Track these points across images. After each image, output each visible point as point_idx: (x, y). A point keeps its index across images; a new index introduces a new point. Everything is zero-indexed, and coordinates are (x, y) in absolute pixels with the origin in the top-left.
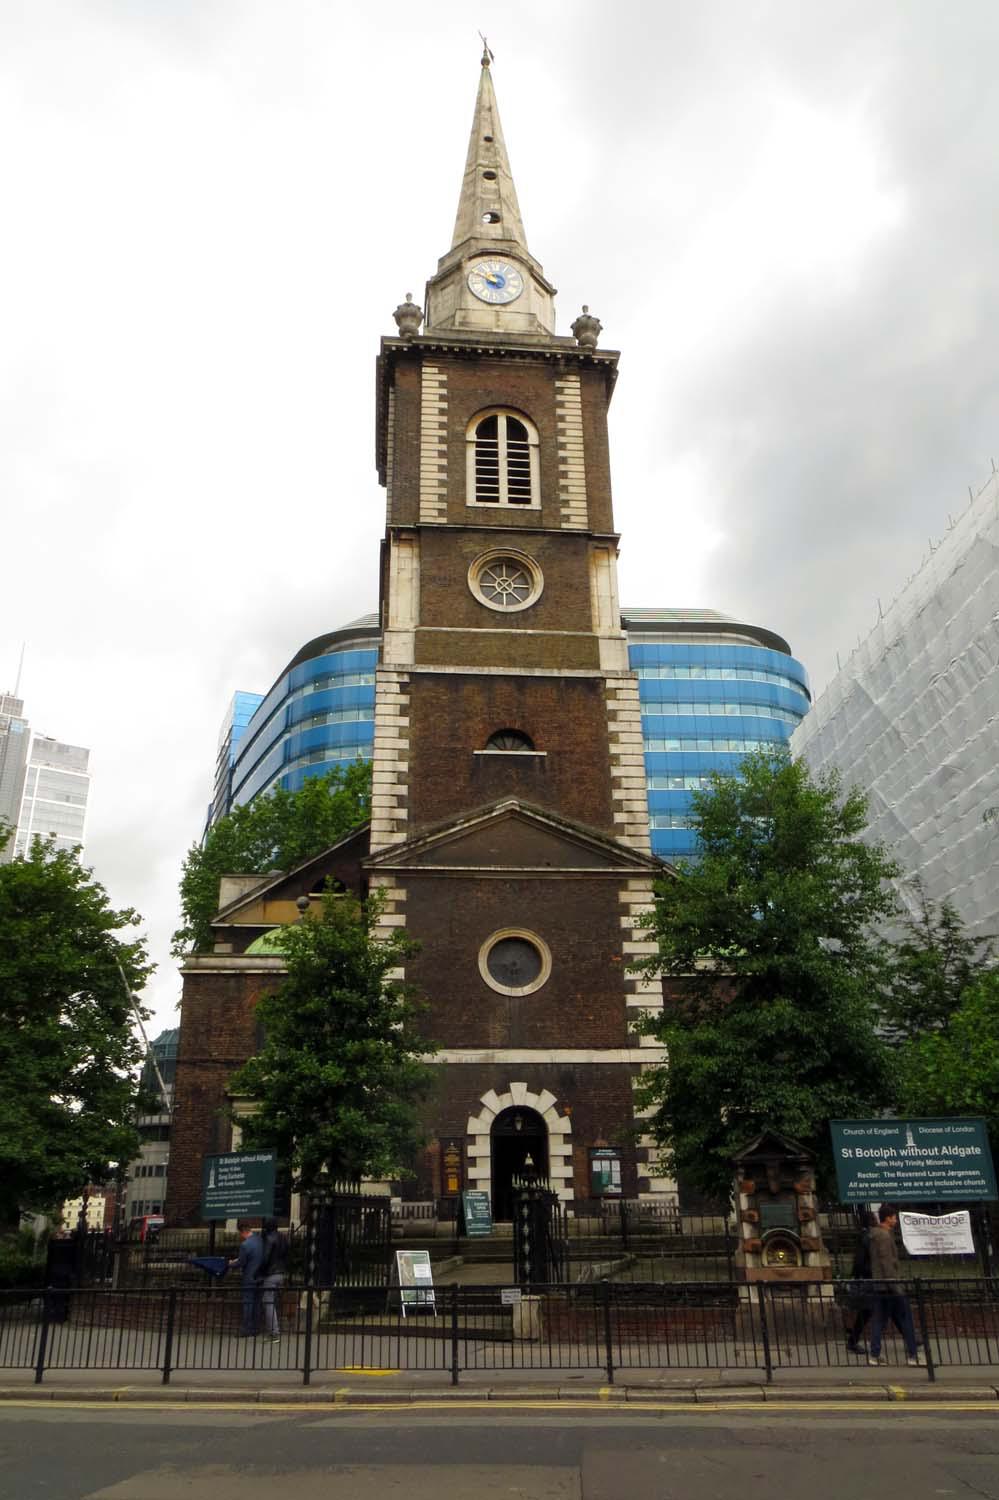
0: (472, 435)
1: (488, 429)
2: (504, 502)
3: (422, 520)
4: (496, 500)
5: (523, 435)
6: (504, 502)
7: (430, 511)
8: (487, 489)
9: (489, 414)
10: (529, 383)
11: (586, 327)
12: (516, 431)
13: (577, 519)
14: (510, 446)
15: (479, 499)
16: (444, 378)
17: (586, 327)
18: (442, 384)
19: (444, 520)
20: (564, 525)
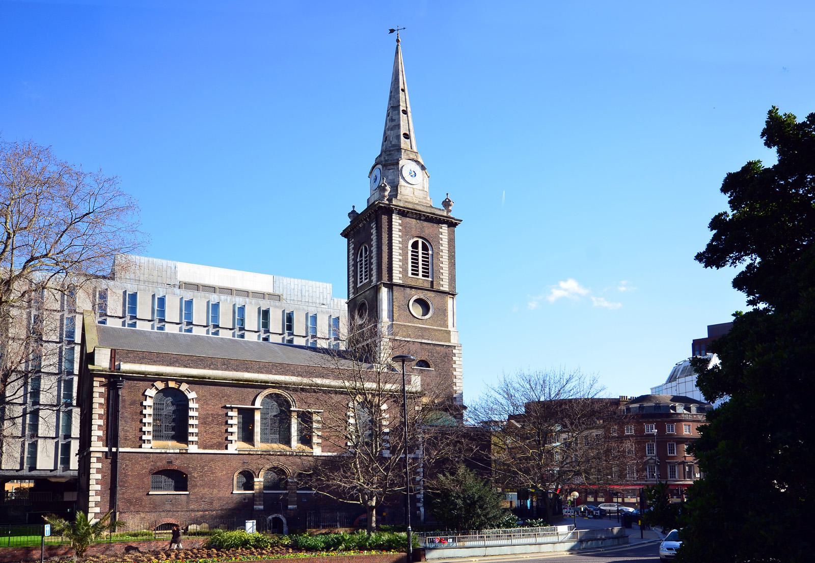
0: (410, 248)
1: (415, 245)
2: (420, 276)
3: (394, 281)
4: (417, 275)
5: (427, 250)
6: (420, 276)
7: (397, 278)
8: (415, 272)
9: (416, 239)
10: (428, 229)
11: (447, 204)
12: (425, 248)
13: (446, 288)
14: (423, 253)
15: (412, 274)
16: (400, 222)
17: (447, 204)
18: (400, 225)
19: (401, 282)
20: (441, 288)
